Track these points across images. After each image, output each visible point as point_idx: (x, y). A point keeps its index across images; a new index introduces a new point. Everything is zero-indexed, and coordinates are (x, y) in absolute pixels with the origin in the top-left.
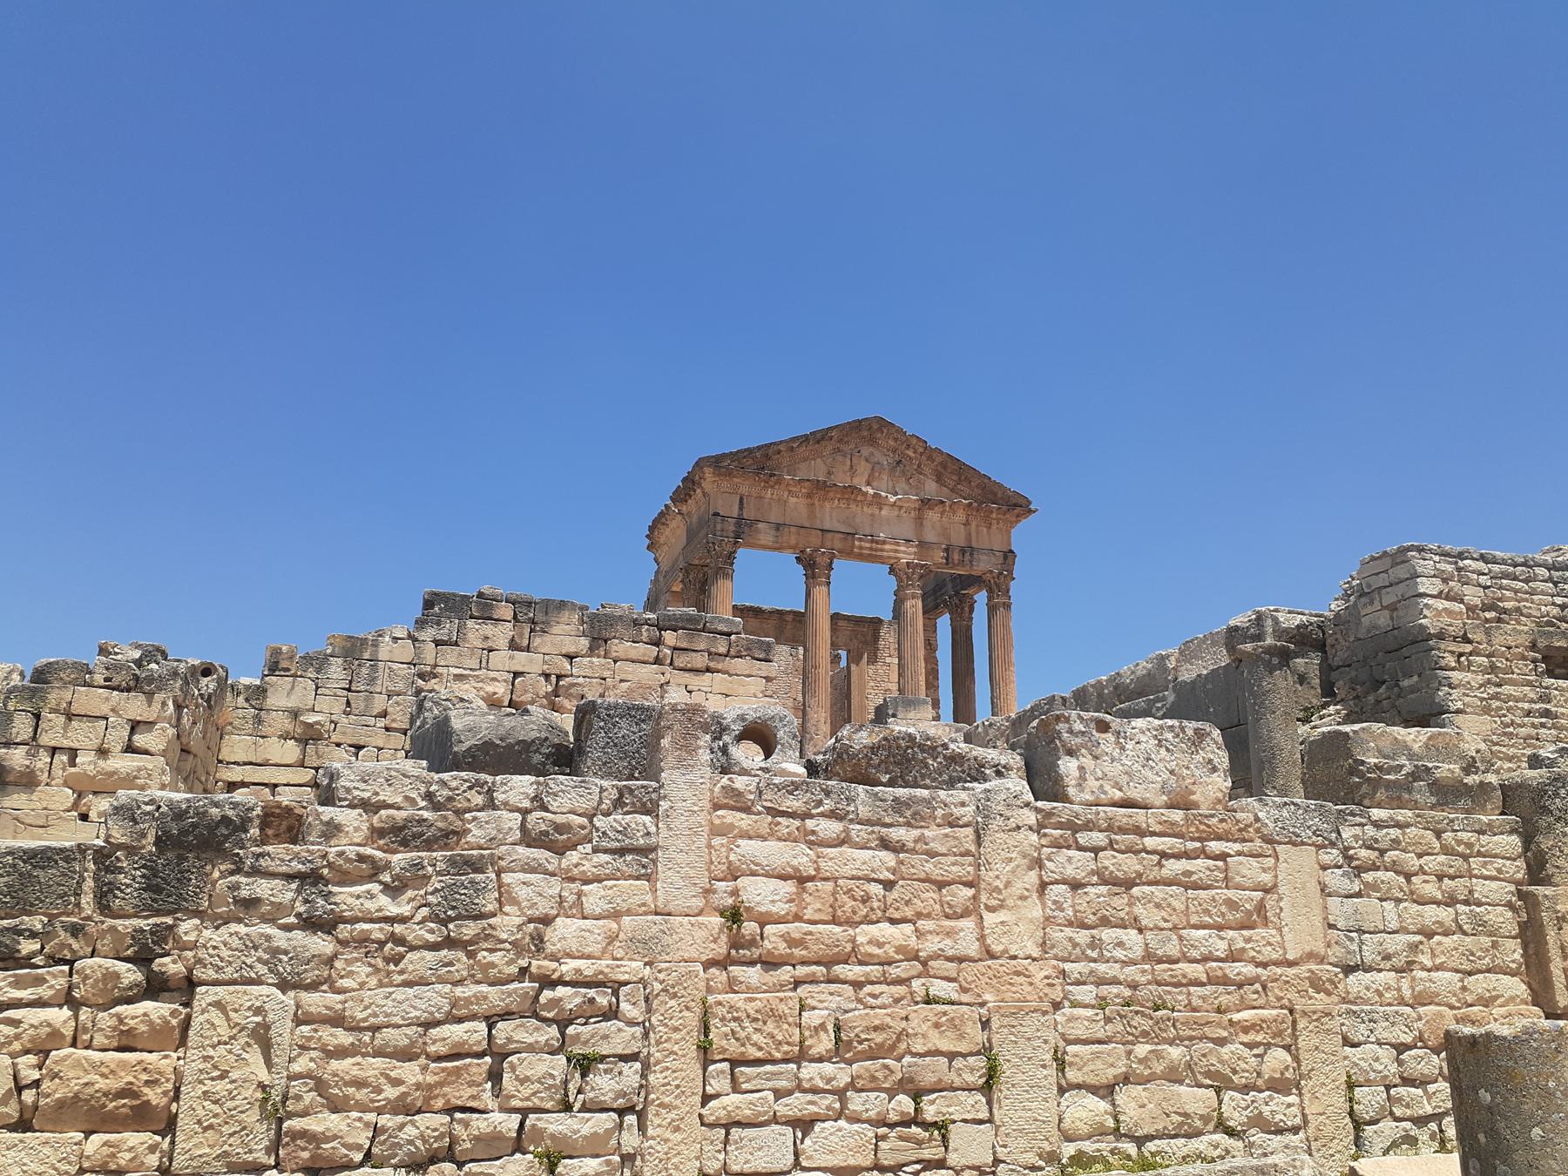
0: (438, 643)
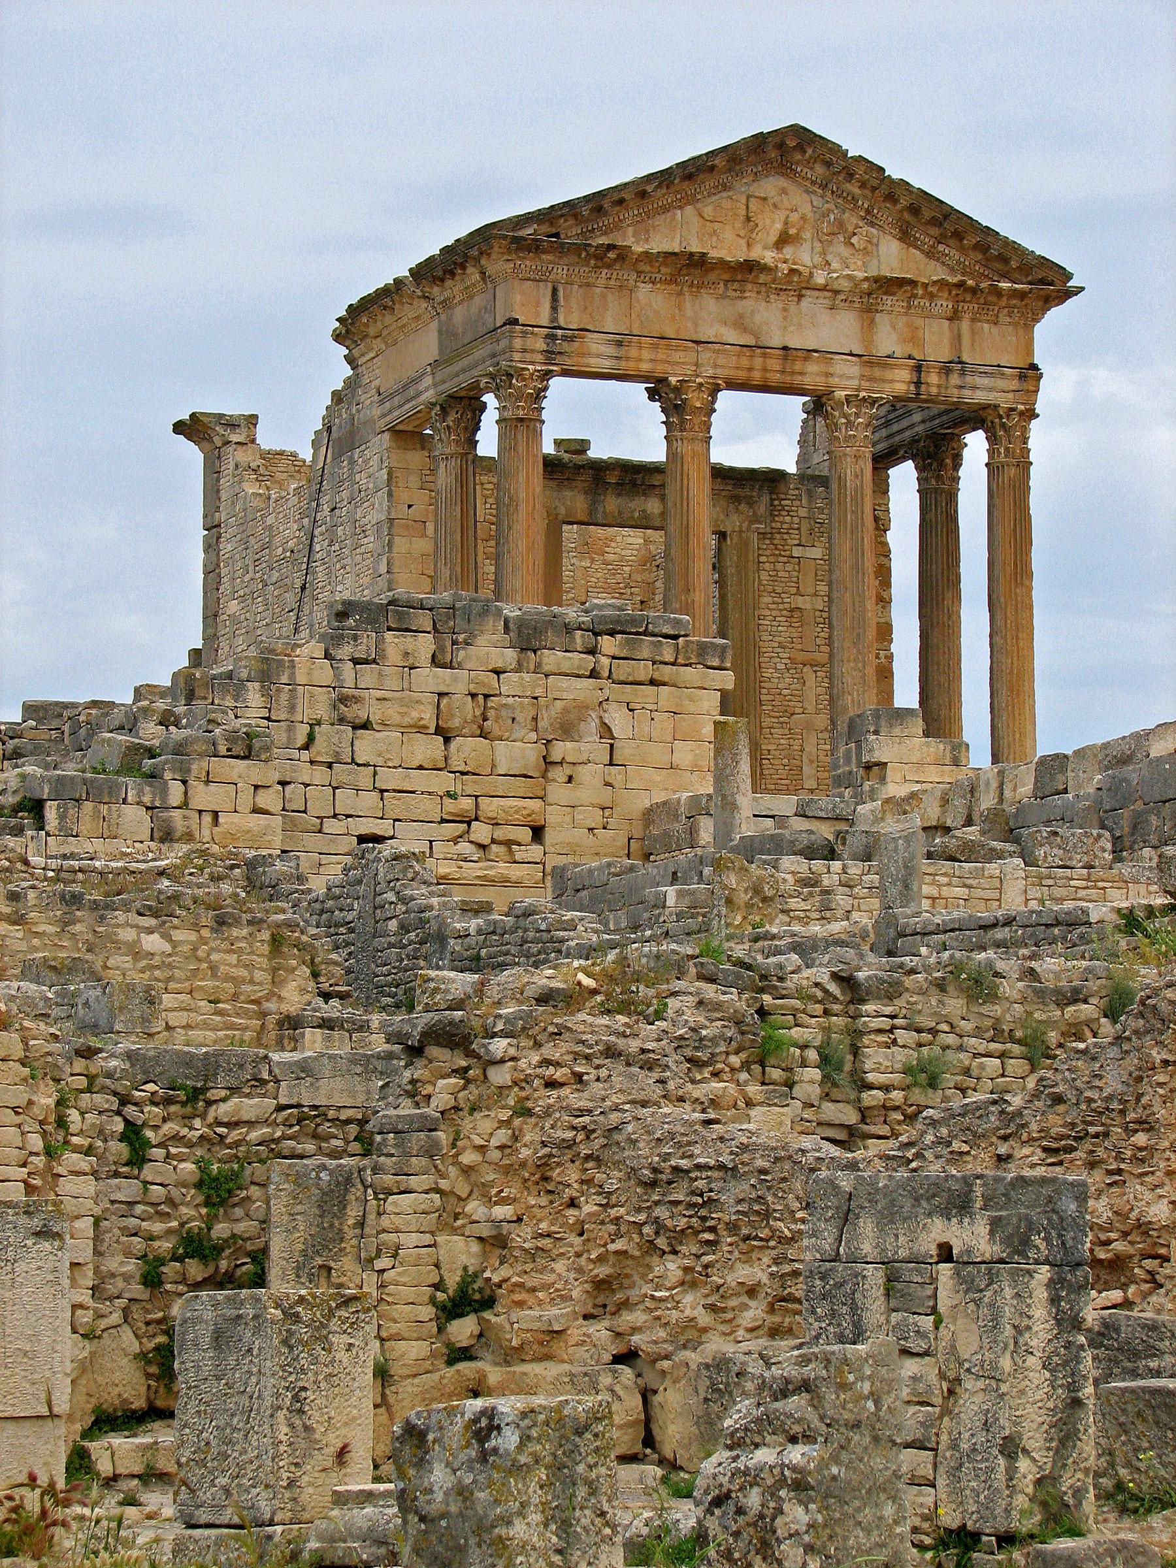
0: (356, 661)
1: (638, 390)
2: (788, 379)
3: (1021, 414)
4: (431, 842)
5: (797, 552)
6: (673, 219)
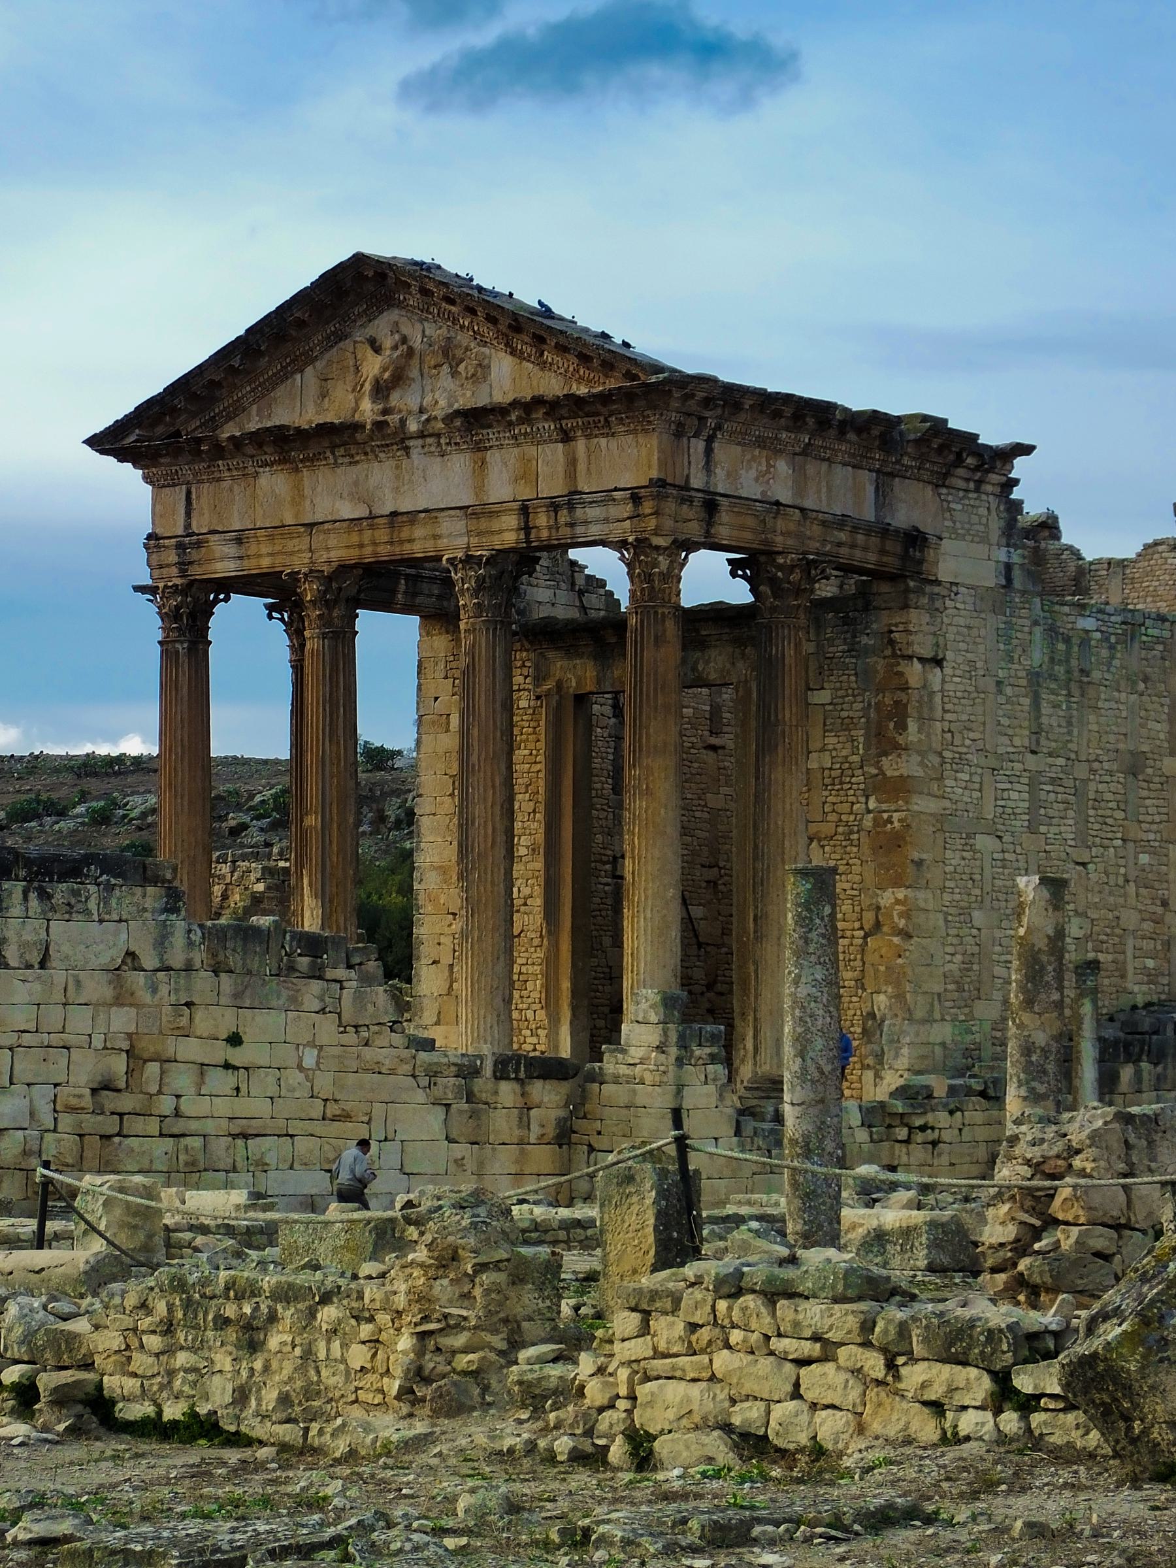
2: (397, 549)
6: (293, 384)
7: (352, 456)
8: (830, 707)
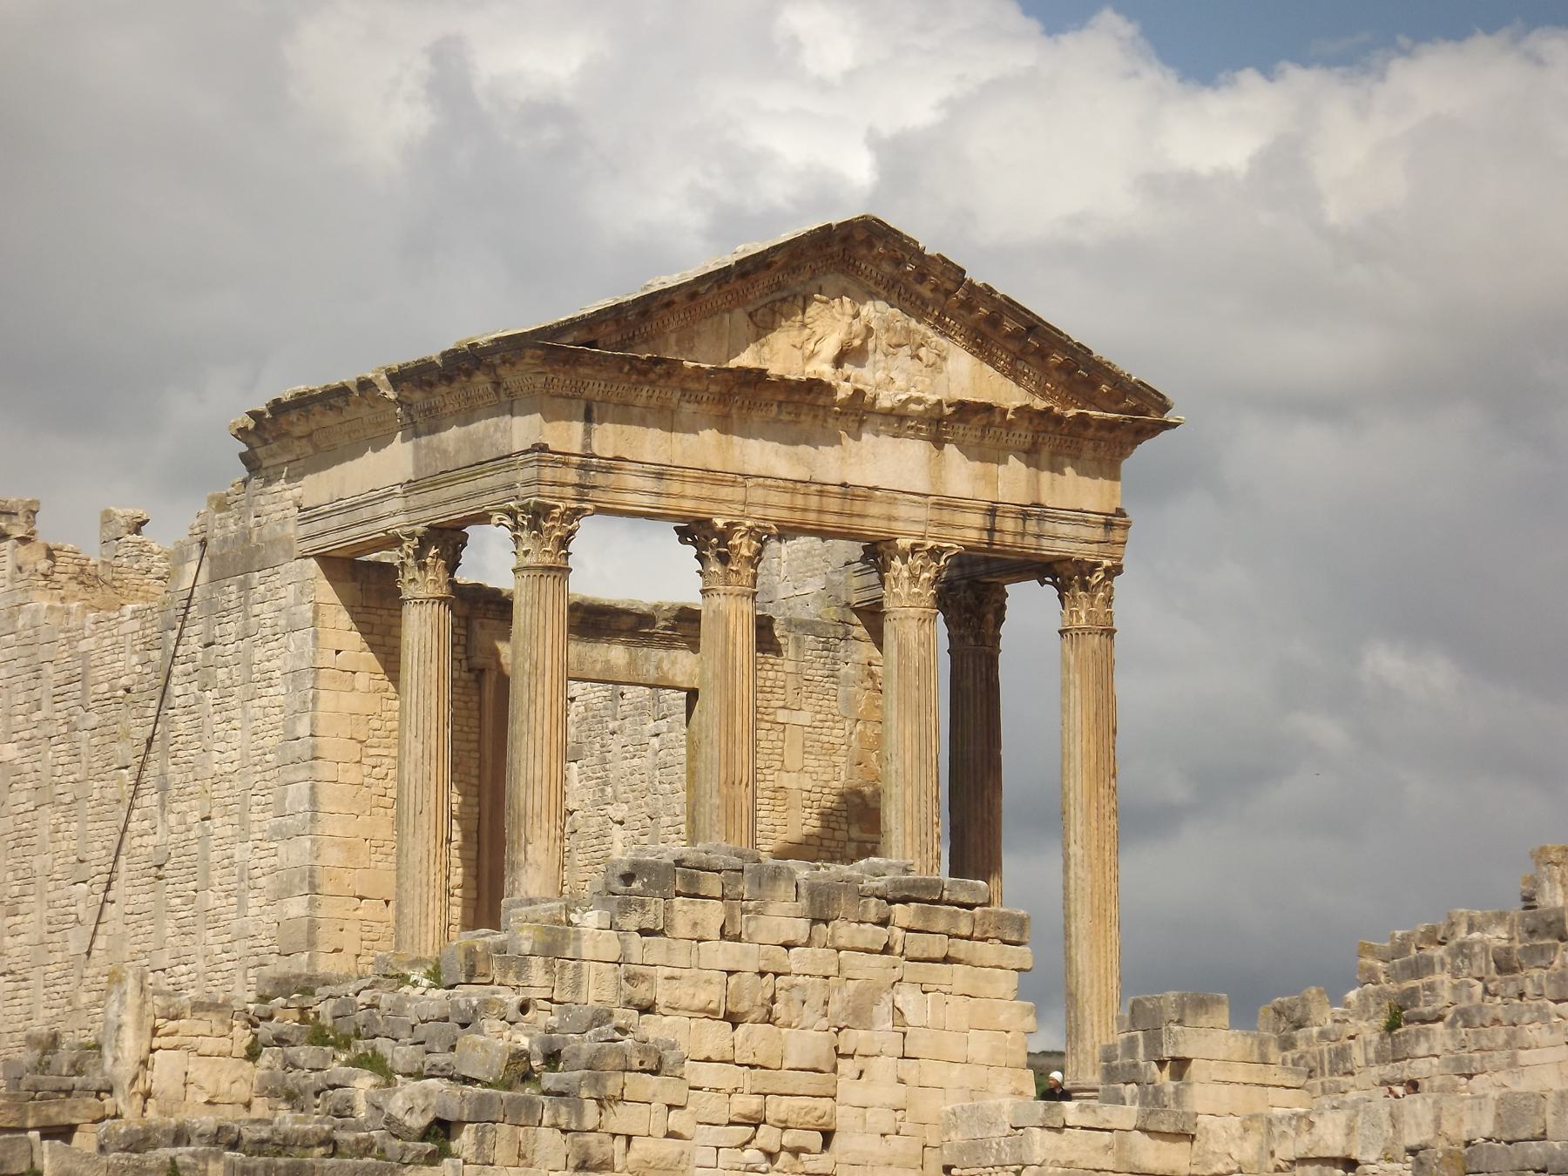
0: (643, 932)
1: (667, 533)
2: (846, 521)
3: (1107, 570)
4: (718, 1148)
5: (782, 716)
7: (798, 415)
8: (810, 729)
